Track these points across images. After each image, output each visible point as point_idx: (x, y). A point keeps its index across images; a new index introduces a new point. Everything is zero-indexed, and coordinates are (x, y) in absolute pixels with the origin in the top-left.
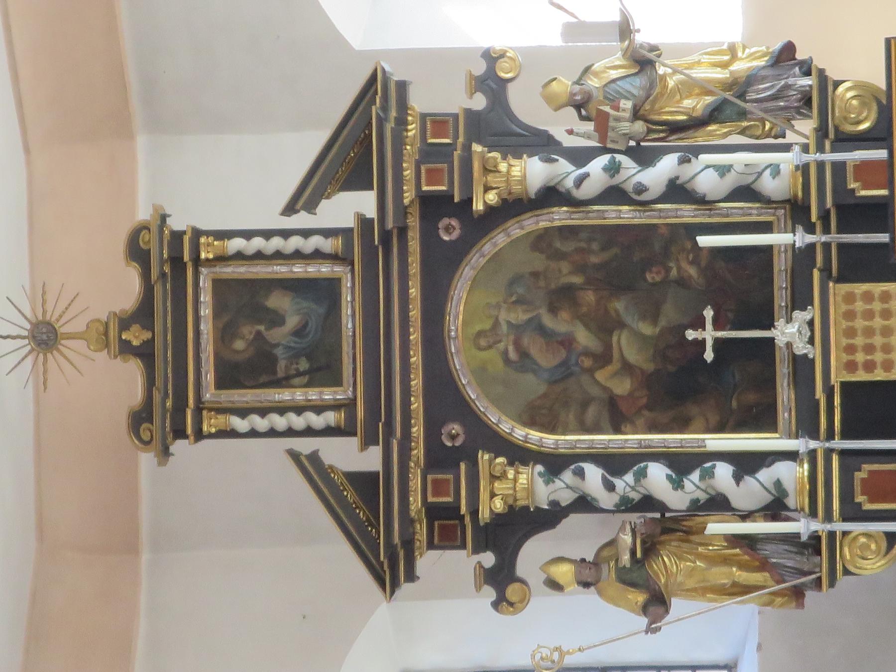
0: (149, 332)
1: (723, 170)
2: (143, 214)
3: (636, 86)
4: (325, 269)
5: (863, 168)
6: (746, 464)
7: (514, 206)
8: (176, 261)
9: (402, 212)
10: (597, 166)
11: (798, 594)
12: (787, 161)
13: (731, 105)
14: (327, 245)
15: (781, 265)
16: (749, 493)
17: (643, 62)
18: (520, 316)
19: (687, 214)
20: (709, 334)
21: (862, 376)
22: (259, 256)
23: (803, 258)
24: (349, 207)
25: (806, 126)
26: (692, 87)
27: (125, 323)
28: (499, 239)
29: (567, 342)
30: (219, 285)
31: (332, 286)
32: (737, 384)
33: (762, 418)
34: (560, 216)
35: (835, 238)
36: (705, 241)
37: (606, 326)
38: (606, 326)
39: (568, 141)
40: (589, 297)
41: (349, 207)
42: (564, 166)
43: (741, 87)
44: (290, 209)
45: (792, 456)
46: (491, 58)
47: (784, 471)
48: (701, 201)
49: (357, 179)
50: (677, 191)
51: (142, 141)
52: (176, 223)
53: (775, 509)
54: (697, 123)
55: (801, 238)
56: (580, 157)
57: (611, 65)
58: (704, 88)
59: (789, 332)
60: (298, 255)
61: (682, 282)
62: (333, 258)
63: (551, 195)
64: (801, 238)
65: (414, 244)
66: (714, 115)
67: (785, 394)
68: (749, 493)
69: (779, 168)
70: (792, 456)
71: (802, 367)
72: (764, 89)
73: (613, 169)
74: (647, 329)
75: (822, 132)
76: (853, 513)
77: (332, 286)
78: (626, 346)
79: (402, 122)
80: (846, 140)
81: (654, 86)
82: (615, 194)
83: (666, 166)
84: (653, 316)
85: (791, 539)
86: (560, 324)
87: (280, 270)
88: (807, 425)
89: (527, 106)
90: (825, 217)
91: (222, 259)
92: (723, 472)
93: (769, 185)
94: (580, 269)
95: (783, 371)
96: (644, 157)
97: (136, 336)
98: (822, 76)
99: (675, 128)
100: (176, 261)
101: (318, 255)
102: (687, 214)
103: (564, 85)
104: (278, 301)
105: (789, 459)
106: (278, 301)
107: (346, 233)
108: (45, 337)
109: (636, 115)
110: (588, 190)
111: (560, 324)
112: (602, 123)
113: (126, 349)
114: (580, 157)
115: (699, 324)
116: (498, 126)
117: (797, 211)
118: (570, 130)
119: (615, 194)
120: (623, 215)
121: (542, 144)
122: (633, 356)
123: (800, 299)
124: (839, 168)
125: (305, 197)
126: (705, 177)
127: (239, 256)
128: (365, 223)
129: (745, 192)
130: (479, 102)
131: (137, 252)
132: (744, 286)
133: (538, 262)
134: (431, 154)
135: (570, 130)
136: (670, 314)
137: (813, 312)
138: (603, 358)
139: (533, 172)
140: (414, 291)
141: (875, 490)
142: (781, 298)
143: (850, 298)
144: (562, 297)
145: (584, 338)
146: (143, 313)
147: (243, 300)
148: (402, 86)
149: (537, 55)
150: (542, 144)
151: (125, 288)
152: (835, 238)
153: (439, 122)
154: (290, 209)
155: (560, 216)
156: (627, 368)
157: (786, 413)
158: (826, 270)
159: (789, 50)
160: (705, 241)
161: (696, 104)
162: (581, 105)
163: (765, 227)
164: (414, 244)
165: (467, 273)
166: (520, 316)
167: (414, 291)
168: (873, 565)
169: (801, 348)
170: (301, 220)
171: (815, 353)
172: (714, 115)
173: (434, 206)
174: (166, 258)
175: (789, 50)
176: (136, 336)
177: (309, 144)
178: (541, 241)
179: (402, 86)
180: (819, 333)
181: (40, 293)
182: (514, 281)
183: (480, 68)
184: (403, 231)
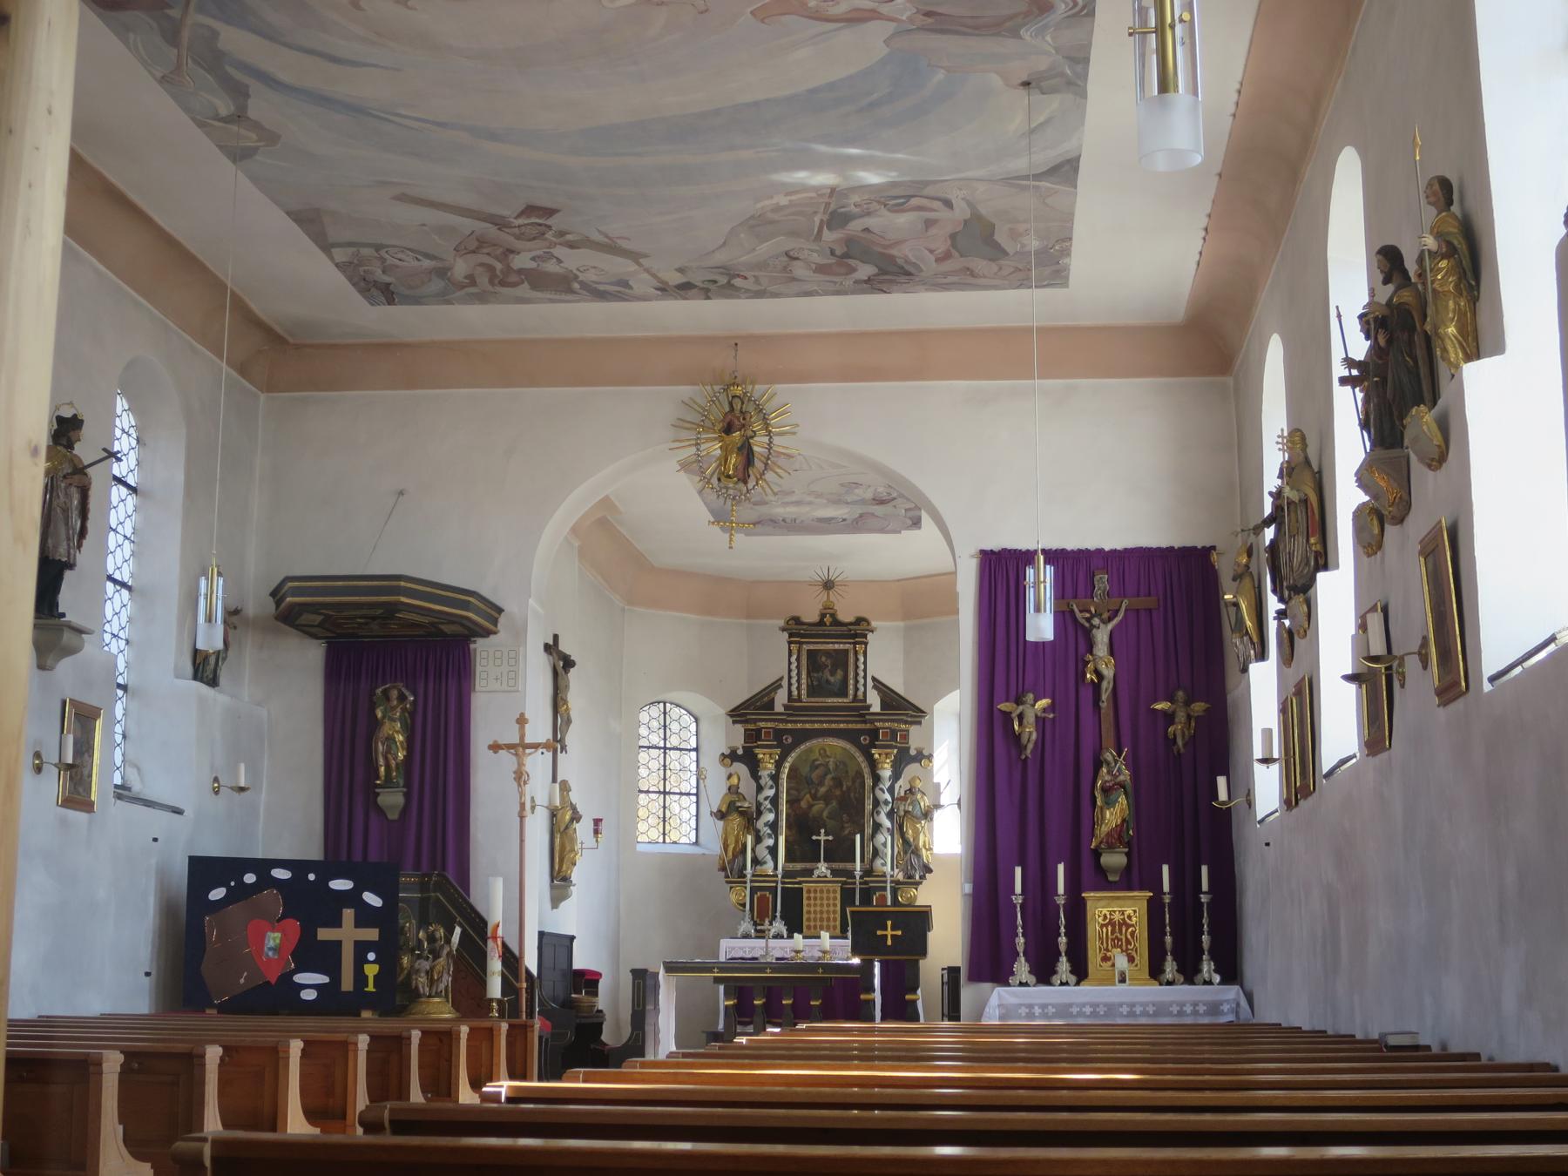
0: (829, 625)
1: (885, 845)
2: (874, 624)
3: (917, 812)
4: (851, 692)
5: (884, 898)
6: (773, 851)
7: (873, 765)
8: (856, 636)
9: (872, 722)
10: (888, 796)
11: (723, 869)
12: (888, 869)
13: (909, 848)
14: (860, 693)
15: (848, 866)
16: (762, 852)
17: (927, 815)
18: (831, 766)
19: (868, 831)
20: (822, 838)
21: (805, 895)
22: (857, 667)
23: (851, 874)
24: (874, 701)
25: (900, 877)
26: (917, 834)
27: (833, 616)
28: (861, 759)
29: (821, 783)
30: (846, 651)
31: (845, 695)
32: (802, 850)
33: (790, 857)
34: (869, 782)
35: (858, 886)
36: (858, 837)
37: (827, 799)
38: (827, 799)
39: (897, 786)
40: (838, 793)
41: (874, 701)
42: (888, 784)
43: (916, 852)
44: (874, 679)
45: (776, 868)
46: (930, 757)
47: (770, 864)
48: (873, 836)
49: (884, 705)
50: (877, 827)
51: (901, 624)
52: (870, 636)
53: (756, 861)
54: (902, 834)
55: (858, 873)
56: (891, 790)
57: (925, 802)
58: (916, 838)
59: (822, 868)
60: (857, 682)
61: (843, 828)
62: (855, 695)
63: (877, 779)
64: (858, 873)
65: (859, 726)
66: (906, 842)
67: (799, 866)
68: (762, 852)
69: (886, 866)
70: (776, 868)
71: (810, 872)
72: (915, 860)
73: (886, 802)
74: (825, 814)
75: (898, 882)
76: (753, 890)
77: (845, 695)
78: (819, 806)
79: (906, 722)
80: (894, 892)
81: (918, 820)
82: (876, 803)
83: (887, 823)
84: (830, 817)
85: (744, 867)
86: (828, 781)
87: (851, 675)
88: (786, 874)
89: (911, 770)
90: (866, 883)
91: (856, 653)
92: (771, 842)
93: (878, 862)
94: (849, 789)
95: (808, 865)
96: (890, 815)
97: (828, 620)
98: (919, 883)
99: (901, 827)
100: (856, 636)
101: (857, 689)
102: (868, 831)
103: (919, 785)
104: (840, 674)
105: (776, 866)
106: (840, 674)
107: (865, 700)
108: (828, 585)
109: (906, 812)
110: (878, 793)
111: (828, 781)
112: (903, 799)
113: (823, 616)
114: (891, 790)
115: (827, 834)
116: (904, 758)
117: (868, 872)
118: (902, 786)
119: (876, 803)
120: (869, 806)
121: (896, 776)
122: (815, 809)
123: (834, 873)
124: (884, 889)
125: (879, 685)
126: (883, 838)
127: (857, 660)
128: (869, 707)
129: (876, 853)
130: (913, 752)
131: (860, 621)
132: (840, 852)
133: (852, 773)
134: (894, 733)
135: (902, 786)
136: (831, 823)
137: (830, 877)
138: (814, 797)
139: (886, 772)
140: (842, 726)
141: (762, 899)
142: (835, 865)
143: (809, 927)
144: (838, 782)
145: (823, 790)
146: (836, 622)
147: (840, 660)
148: (919, 723)
149: (930, 774)
150: (896, 776)
151: (846, 616)
152: (858, 886)
153: (905, 737)
154: (874, 679)
155: (869, 782)
156: (811, 806)
157: (791, 866)
158: (844, 883)
159: (930, 871)
160: (858, 837)
161: (910, 834)
162: (911, 791)
163: (862, 860)
164: (859, 726)
165: (848, 746)
166: (831, 766)
167: (842, 726)
168: (733, 898)
169: (816, 873)
170: (870, 683)
171: (814, 878)
172: (906, 842)
173: (874, 734)
174: (857, 631)
175: (930, 871)
176: (828, 620)
177: (899, 688)
178: (860, 774)
179: (919, 723)
180: (822, 880)
181: (845, 584)
182: (845, 764)
183: (926, 753)
184: (865, 722)
